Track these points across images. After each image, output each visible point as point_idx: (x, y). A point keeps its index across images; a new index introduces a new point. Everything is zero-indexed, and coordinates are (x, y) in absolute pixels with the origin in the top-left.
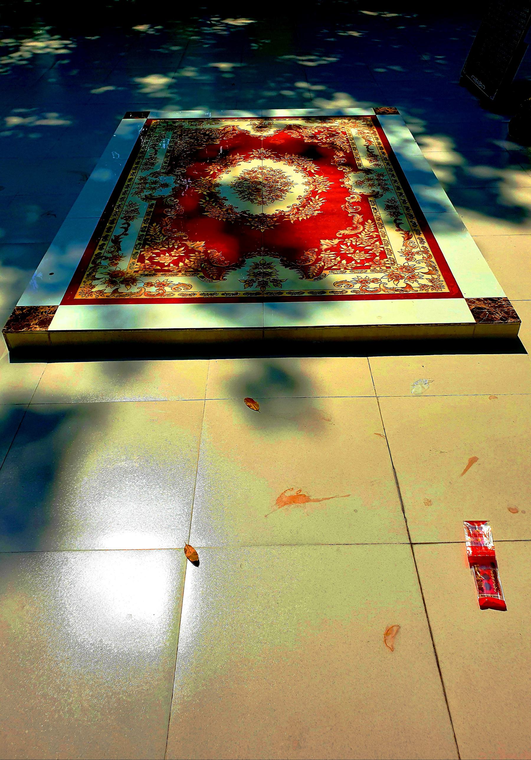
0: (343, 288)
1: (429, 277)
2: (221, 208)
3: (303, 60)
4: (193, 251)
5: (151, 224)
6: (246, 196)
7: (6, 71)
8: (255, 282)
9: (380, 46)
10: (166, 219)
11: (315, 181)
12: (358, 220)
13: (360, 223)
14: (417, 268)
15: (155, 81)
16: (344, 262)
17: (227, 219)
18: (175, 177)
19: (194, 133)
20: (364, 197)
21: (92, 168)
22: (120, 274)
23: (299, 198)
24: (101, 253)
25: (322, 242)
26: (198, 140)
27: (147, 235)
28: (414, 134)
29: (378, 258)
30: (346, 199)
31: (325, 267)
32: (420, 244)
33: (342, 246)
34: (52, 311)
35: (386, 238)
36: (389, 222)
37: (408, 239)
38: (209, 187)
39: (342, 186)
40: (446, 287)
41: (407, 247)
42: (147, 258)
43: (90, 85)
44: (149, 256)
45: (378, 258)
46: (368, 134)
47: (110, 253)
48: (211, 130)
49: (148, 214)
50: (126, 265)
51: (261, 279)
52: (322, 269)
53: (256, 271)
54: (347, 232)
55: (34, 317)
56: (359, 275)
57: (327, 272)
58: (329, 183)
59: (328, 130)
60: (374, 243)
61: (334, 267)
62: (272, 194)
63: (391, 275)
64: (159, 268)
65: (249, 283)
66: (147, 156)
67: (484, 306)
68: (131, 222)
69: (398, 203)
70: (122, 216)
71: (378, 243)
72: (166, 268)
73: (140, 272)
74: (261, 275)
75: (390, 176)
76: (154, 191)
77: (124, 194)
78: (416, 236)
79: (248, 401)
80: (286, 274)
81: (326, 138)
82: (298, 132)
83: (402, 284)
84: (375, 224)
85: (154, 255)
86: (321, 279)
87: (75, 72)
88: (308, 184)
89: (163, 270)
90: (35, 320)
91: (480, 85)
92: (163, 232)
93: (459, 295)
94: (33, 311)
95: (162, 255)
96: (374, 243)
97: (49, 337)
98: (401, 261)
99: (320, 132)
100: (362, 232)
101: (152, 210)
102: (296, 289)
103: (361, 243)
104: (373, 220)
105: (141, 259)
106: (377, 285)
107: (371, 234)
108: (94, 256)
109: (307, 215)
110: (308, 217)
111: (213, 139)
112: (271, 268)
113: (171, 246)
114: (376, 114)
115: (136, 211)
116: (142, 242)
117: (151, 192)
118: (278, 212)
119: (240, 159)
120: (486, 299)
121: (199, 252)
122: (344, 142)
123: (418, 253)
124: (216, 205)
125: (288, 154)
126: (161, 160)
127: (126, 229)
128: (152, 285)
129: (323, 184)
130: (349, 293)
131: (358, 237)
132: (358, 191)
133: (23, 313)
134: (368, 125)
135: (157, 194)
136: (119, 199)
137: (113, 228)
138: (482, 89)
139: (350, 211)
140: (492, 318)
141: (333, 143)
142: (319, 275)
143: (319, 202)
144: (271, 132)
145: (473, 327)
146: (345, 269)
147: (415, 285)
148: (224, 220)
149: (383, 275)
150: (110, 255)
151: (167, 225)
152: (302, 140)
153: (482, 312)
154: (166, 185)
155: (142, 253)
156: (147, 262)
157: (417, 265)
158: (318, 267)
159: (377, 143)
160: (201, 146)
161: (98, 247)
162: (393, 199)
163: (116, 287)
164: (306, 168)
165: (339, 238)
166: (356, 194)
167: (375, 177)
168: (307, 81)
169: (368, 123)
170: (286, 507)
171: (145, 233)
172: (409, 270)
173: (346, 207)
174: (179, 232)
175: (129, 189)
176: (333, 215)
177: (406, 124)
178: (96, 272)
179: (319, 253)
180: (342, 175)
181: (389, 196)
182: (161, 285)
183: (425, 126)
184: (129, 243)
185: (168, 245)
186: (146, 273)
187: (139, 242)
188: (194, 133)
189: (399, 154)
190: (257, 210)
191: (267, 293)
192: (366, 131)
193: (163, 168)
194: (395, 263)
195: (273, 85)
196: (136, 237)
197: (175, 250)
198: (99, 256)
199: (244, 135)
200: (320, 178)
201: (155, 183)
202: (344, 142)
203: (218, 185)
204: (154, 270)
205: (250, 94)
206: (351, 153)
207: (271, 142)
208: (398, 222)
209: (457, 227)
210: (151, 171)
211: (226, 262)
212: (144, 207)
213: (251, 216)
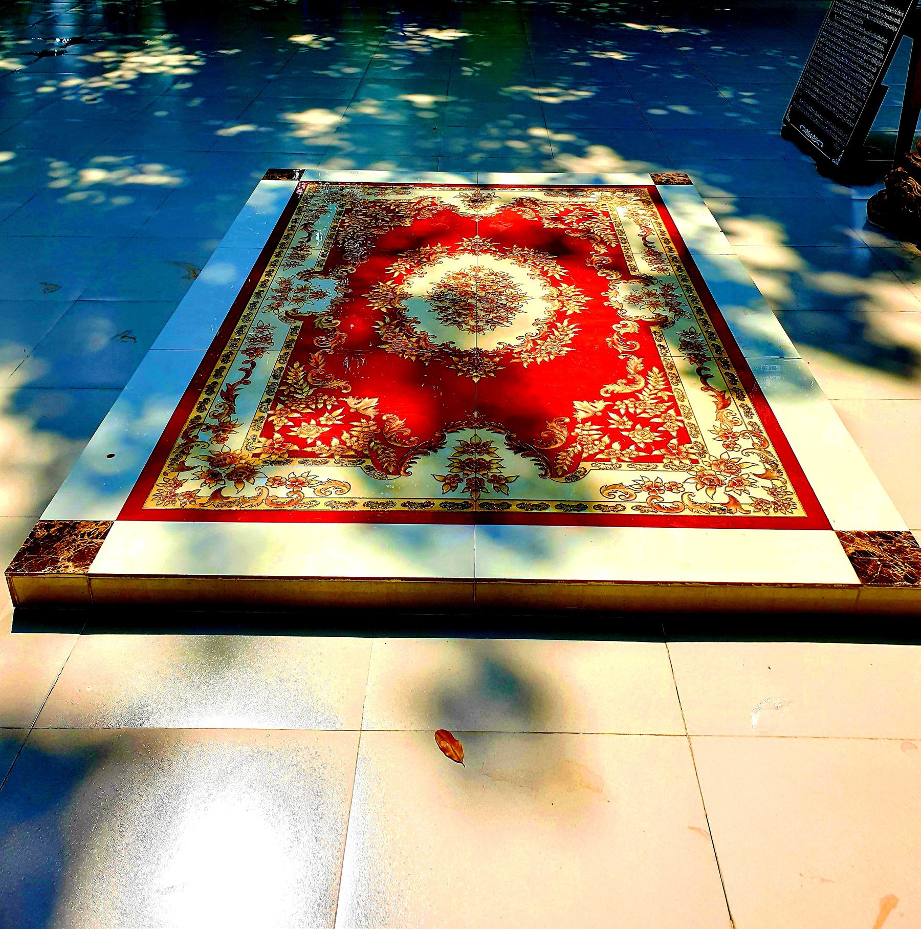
0: (617, 499)
1: (767, 483)
2: (408, 337)
3: (539, 95)
4: (357, 416)
5: (290, 364)
6: (450, 317)
7: (95, 99)
8: (461, 480)
9: (655, 75)
10: (317, 354)
11: (561, 295)
12: (636, 367)
13: (640, 373)
14: (746, 465)
15: (316, 122)
16: (616, 446)
17: (417, 357)
18: (337, 282)
19: (372, 207)
20: (644, 326)
21: (206, 259)
22: (228, 460)
25: (577, 404)
26: (377, 220)
27: (282, 384)
28: (718, 216)
29: (674, 441)
30: (614, 327)
31: (584, 455)
32: (745, 418)
33: (611, 415)
34: (100, 533)
35: (686, 403)
36: (688, 373)
39: (606, 304)
40: (799, 505)
41: (722, 421)
42: (277, 429)
43: (218, 123)
44: (281, 424)
45: (674, 441)
46: (644, 217)
47: (215, 417)
48: (399, 204)
49: (287, 345)
52: (578, 458)
53: (464, 457)
54: (619, 387)
55: (69, 543)
58: (584, 299)
59: (581, 209)
60: (665, 412)
61: (599, 456)
62: (492, 315)
63: (700, 477)
64: (296, 448)
65: (450, 482)
67: (871, 549)
68: (257, 360)
69: (702, 338)
70: (244, 348)
71: (672, 412)
72: (309, 449)
73: (263, 456)
74: (472, 467)
75: (685, 289)
76: (301, 304)
78: (737, 400)
79: (444, 739)
80: (515, 465)
81: (578, 221)
84: (665, 375)
85: (291, 423)
86: (578, 478)
87: (196, 102)
89: (303, 452)
90: (69, 550)
91: (814, 139)
92: (309, 380)
95: (303, 424)
96: (665, 412)
97: (89, 585)
98: (716, 449)
99: (567, 212)
100: (643, 389)
101: (296, 338)
102: (534, 497)
103: (644, 412)
104: (661, 369)
105: (268, 431)
107: (659, 394)
108: (188, 423)
109: (549, 354)
110: (552, 357)
112: (489, 453)
113: (320, 406)
114: (657, 183)
115: (266, 339)
116: (272, 398)
117: (295, 306)
118: (501, 347)
119: (442, 252)
120: (873, 534)
121: (368, 418)
122: (606, 230)
124: (400, 331)
125: (519, 246)
126: (317, 251)
127: (248, 373)
128: (281, 484)
129: (575, 301)
130: (629, 511)
131: (638, 399)
134: (643, 201)
135: (305, 309)
139: (621, 349)
140: (889, 574)
141: (588, 231)
142: (573, 473)
143: (567, 331)
144: (490, 210)
145: (855, 592)
146: (619, 460)
147: (743, 499)
148: (413, 358)
150: (215, 422)
151: (317, 365)
152: (539, 224)
153: (870, 562)
154: (319, 295)
155: (270, 419)
156: (277, 435)
158: (572, 455)
160: (381, 228)
161: (196, 406)
162: (692, 330)
163: (218, 487)
164: (547, 271)
165: (606, 399)
166: (629, 318)
167: (659, 291)
168: (546, 128)
173: (613, 343)
174: (335, 379)
176: (591, 359)
177: (703, 197)
178: (188, 454)
179: (572, 426)
180: (604, 285)
181: (684, 324)
182: (297, 483)
183: (735, 204)
184: (250, 399)
185: (316, 403)
186: (273, 458)
187: (269, 397)
188: (372, 207)
189: (698, 253)
190: (467, 342)
191: (482, 505)
192: (641, 212)
193: (319, 264)
194: (705, 452)
195: (494, 131)
196: (264, 388)
197: (327, 414)
198: (196, 423)
199: (448, 213)
201: (304, 289)
202: (606, 230)
203: (405, 296)
204: (288, 451)
205: (458, 145)
206: (618, 246)
207: (491, 226)
208: (704, 373)
211: (412, 439)
212: (282, 332)
213: (457, 352)
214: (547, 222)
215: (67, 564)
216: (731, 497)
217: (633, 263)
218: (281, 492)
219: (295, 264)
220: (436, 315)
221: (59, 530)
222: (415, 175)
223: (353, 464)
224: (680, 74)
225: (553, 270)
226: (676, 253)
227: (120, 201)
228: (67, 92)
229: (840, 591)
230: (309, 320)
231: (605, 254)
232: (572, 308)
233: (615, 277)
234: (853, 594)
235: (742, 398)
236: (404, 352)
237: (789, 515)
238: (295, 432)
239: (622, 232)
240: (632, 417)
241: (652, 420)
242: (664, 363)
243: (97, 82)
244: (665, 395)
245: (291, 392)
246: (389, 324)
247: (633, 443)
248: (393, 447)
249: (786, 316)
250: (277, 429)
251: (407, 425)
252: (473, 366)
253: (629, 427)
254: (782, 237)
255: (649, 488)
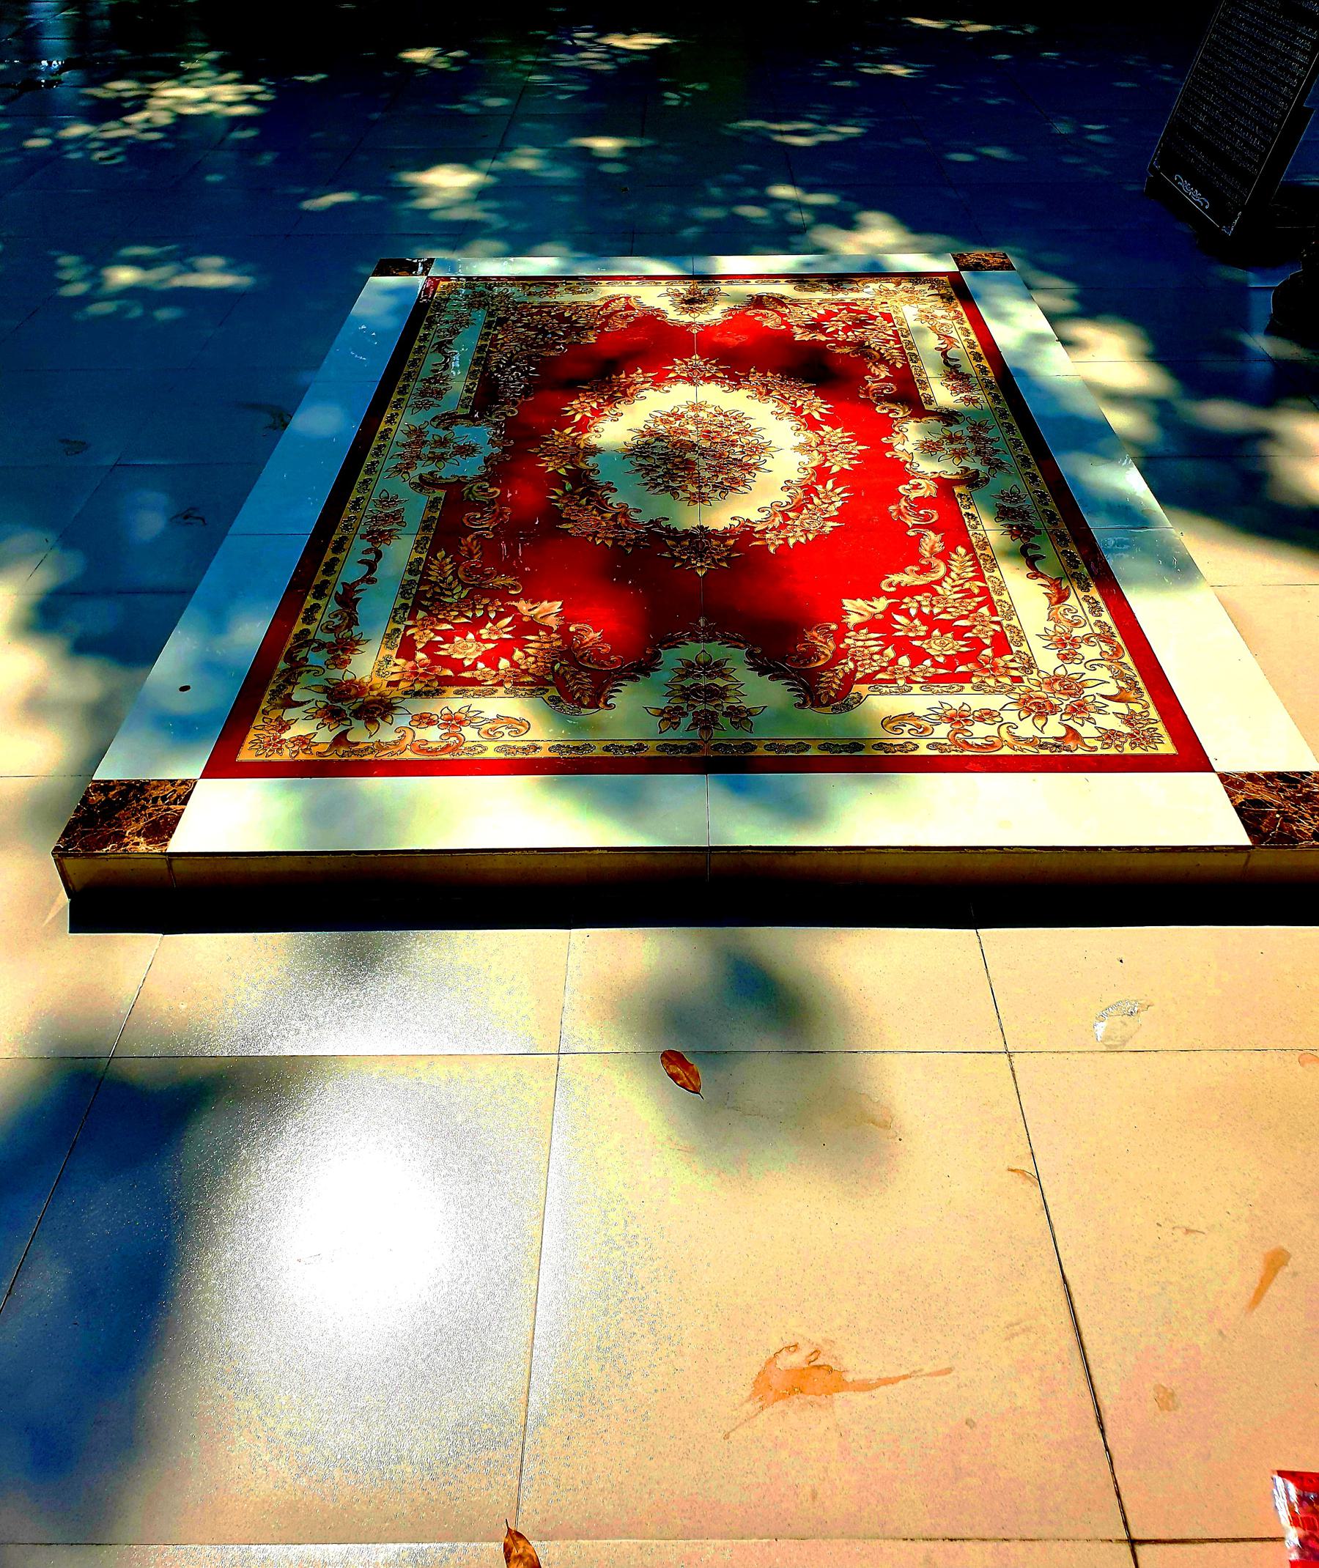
0: (906, 735)
1: (1122, 708)
2: (601, 512)
3: (782, 133)
4: (533, 627)
6: (660, 481)
8: (685, 714)
9: (956, 99)
10: (469, 539)
11: (822, 443)
12: (933, 547)
13: (938, 556)
14: (1090, 683)
15: (448, 182)
16: (904, 661)
17: (615, 540)
19: (537, 314)
20: (944, 485)
22: (353, 692)
23: (787, 486)
24: (308, 631)
25: (848, 604)
26: (546, 333)
27: (422, 582)
28: (1052, 318)
29: (988, 652)
30: (900, 489)
31: (859, 675)
32: (1090, 616)
33: (897, 618)
34: (179, 797)
35: (1005, 597)
36: (1009, 554)
37: (1059, 602)
38: (572, 456)
39: (888, 455)
40: (1167, 739)
41: (1058, 622)
42: (420, 646)
43: (302, 190)
44: (425, 640)
45: (988, 652)
46: (943, 321)
47: (331, 631)
48: (575, 307)
49: (426, 526)
50: (369, 665)
51: (700, 707)
52: (849, 680)
53: (688, 682)
54: (907, 578)
56: (944, 698)
57: (863, 689)
58: (857, 448)
59: (850, 311)
60: (976, 609)
61: (880, 676)
62: (721, 476)
63: (1025, 702)
64: (449, 673)
65: (670, 716)
66: (426, 372)
67: (1268, 798)
68: (382, 547)
69: (1029, 502)
70: (362, 531)
71: (984, 610)
72: (467, 674)
73: (402, 685)
74: (699, 695)
76: (441, 464)
77: (368, 472)
78: (1078, 591)
79: (673, 1063)
80: (761, 692)
81: (846, 330)
82: (778, 313)
83: (1054, 727)
84: (975, 558)
85: (439, 638)
86: (849, 708)
87: (267, 158)
88: (805, 448)
89: (460, 679)
90: (137, 821)
93: (1203, 765)
94: (134, 792)
95: (457, 639)
96: (976, 609)
97: (170, 868)
98: (1048, 661)
99: (830, 314)
100: (943, 579)
101: (437, 515)
102: (789, 735)
103: (945, 611)
104: (970, 549)
105: (407, 650)
106: (992, 730)
107: (967, 586)
108: (291, 640)
109: (806, 532)
110: (811, 537)
111: (579, 331)
112: (724, 676)
113: (479, 614)
114: (961, 268)
115: (396, 517)
116: (410, 602)
117: (432, 467)
118: (736, 523)
119: (644, 382)
120: (1270, 776)
121: (548, 630)
122: (888, 341)
123: (1087, 640)
124: (588, 503)
125: (758, 370)
126: (459, 383)
127: (372, 567)
128: (431, 723)
129: (844, 451)
130: (923, 751)
131: (935, 593)
132: (928, 467)
133: (108, 800)
134: (942, 296)
135: (447, 472)
136: (357, 486)
137: (340, 564)
138: (1203, 208)
139: (911, 521)
140: (1292, 831)
141: (861, 343)
142: (843, 700)
143: (833, 498)
144: (714, 314)
145: (1243, 856)
146: (909, 681)
147: (1087, 730)
148: (609, 543)
149: (1003, 699)
150: (330, 638)
151: (471, 555)
152: (788, 334)
153: (1265, 814)
155: (409, 633)
156: (420, 656)
157: (1089, 675)
158: (841, 675)
159: (966, 344)
161: (302, 616)
164: (801, 407)
165: (889, 595)
168: (793, 183)
169: (943, 291)
170: (780, 1405)
171: (417, 578)
172: (1070, 688)
173: (900, 513)
174: (499, 574)
175: (381, 459)
176: (869, 536)
179: (840, 635)
180: (886, 426)
181: (1005, 482)
182: (454, 722)
183: (1076, 298)
184: (378, 605)
185: (474, 609)
186: (418, 687)
187: (404, 601)
188: (537, 314)
189: (1022, 373)
190: (688, 517)
191: (716, 748)
192: (939, 313)
195: (716, 192)
196: (396, 589)
197: (490, 625)
199: (651, 320)
200: (835, 435)
201: (443, 443)
202: (888, 341)
203: (593, 451)
205: (663, 215)
206: (906, 367)
207: (715, 339)
208: (1030, 552)
209: (1180, 569)
210: (433, 412)
212: (416, 507)
213: (672, 533)
214: (799, 331)
215: (137, 839)
216: (1069, 728)
217: (928, 391)
218: (432, 735)
219: (427, 406)
220: (638, 478)
221: (120, 793)
222: (603, 261)
223: (531, 694)
224: (994, 97)
225: (810, 406)
226: (991, 374)
227: (164, 314)
228: (69, 147)
229: (1221, 856)
230: (455, 487)
231: (887, 379)
232: (839, 463)
233: (901, 415)
234: (1240, 859)
235: (1086, 588)
236: (595, 534)
237: (1151, 751)
238: (446, 650)
239: (911, 345)
240: (927, 619)
241: (957, 623)
242: (974, 540)
243: (114, 130)
244: (975, 586)
245: (435, 593)
246: (571, 492)
247: (929, 656)
248: (587, 670)
249: (1150, 466)
250: (420, 646)
251: (605, 639)
252: (697, 552)
253: (922, 634)
254: (1148, 347)
255: (951, 719)
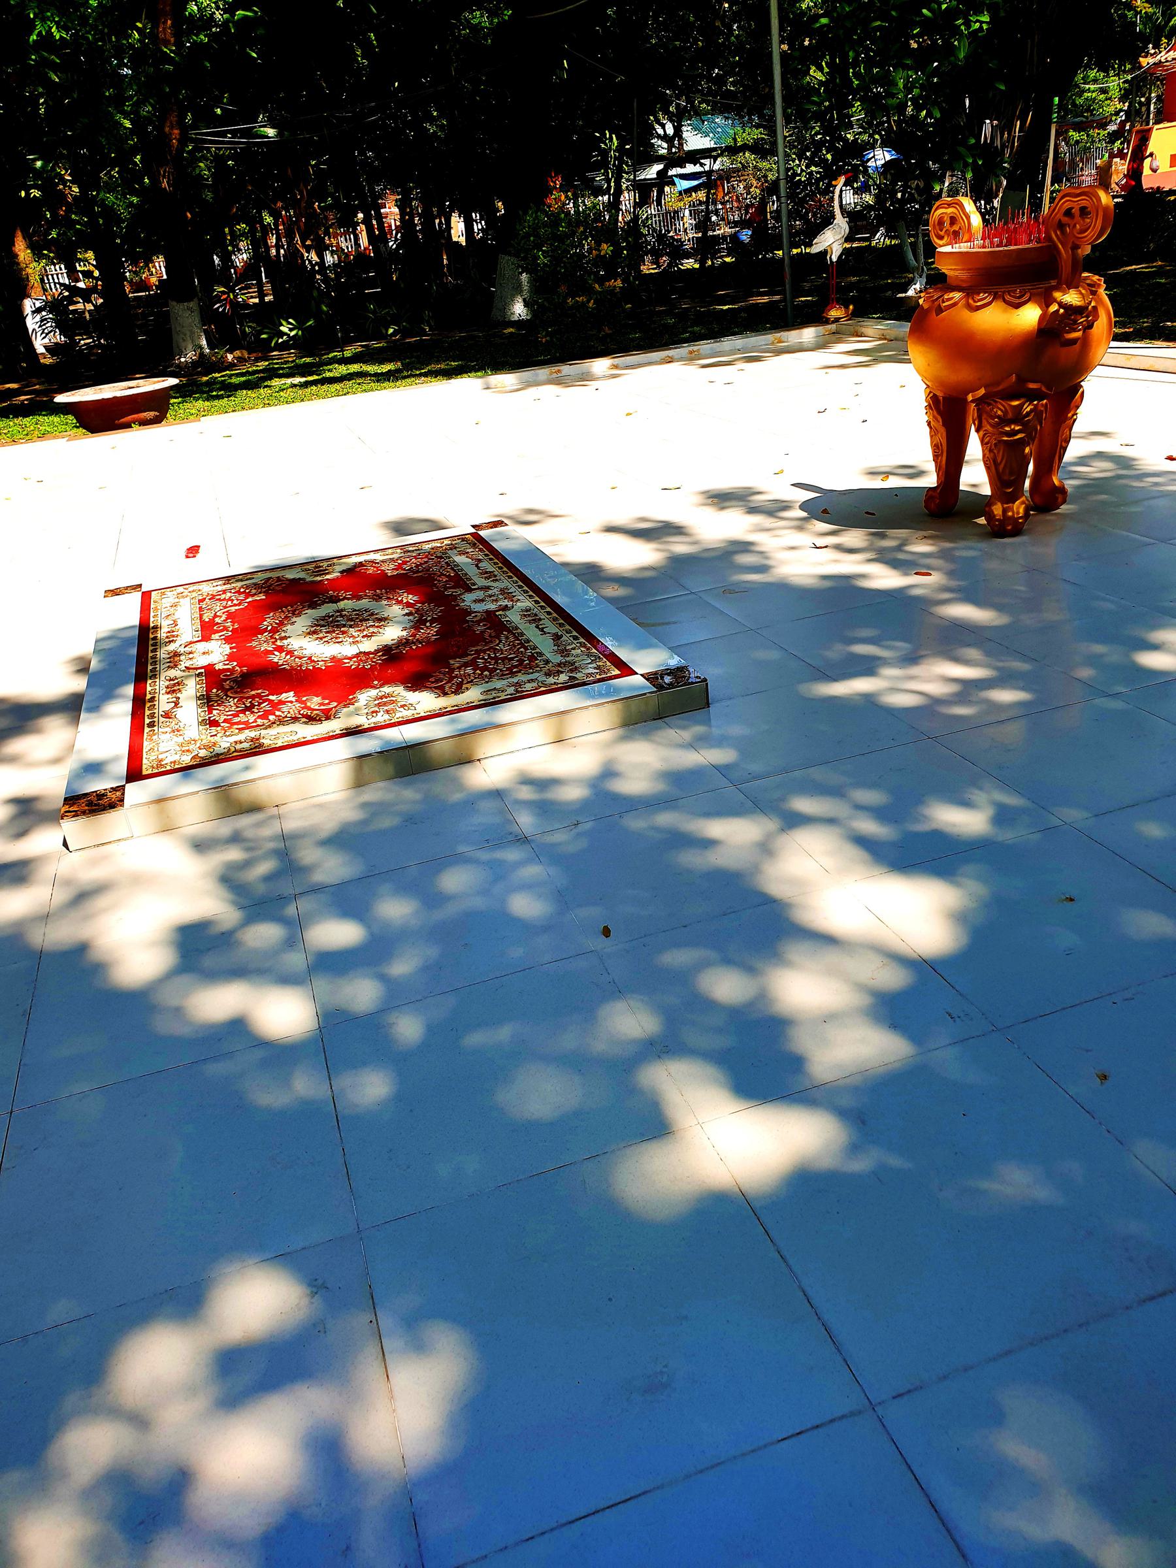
25: (452, 662)
57: (468, 685)
68: (179, 695)
104: (509, 631)
238: (236, 720)
